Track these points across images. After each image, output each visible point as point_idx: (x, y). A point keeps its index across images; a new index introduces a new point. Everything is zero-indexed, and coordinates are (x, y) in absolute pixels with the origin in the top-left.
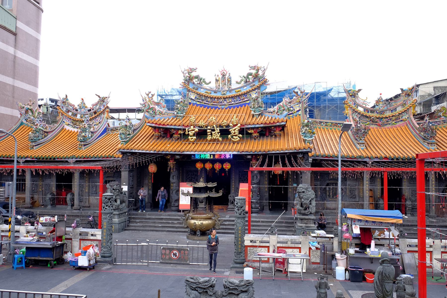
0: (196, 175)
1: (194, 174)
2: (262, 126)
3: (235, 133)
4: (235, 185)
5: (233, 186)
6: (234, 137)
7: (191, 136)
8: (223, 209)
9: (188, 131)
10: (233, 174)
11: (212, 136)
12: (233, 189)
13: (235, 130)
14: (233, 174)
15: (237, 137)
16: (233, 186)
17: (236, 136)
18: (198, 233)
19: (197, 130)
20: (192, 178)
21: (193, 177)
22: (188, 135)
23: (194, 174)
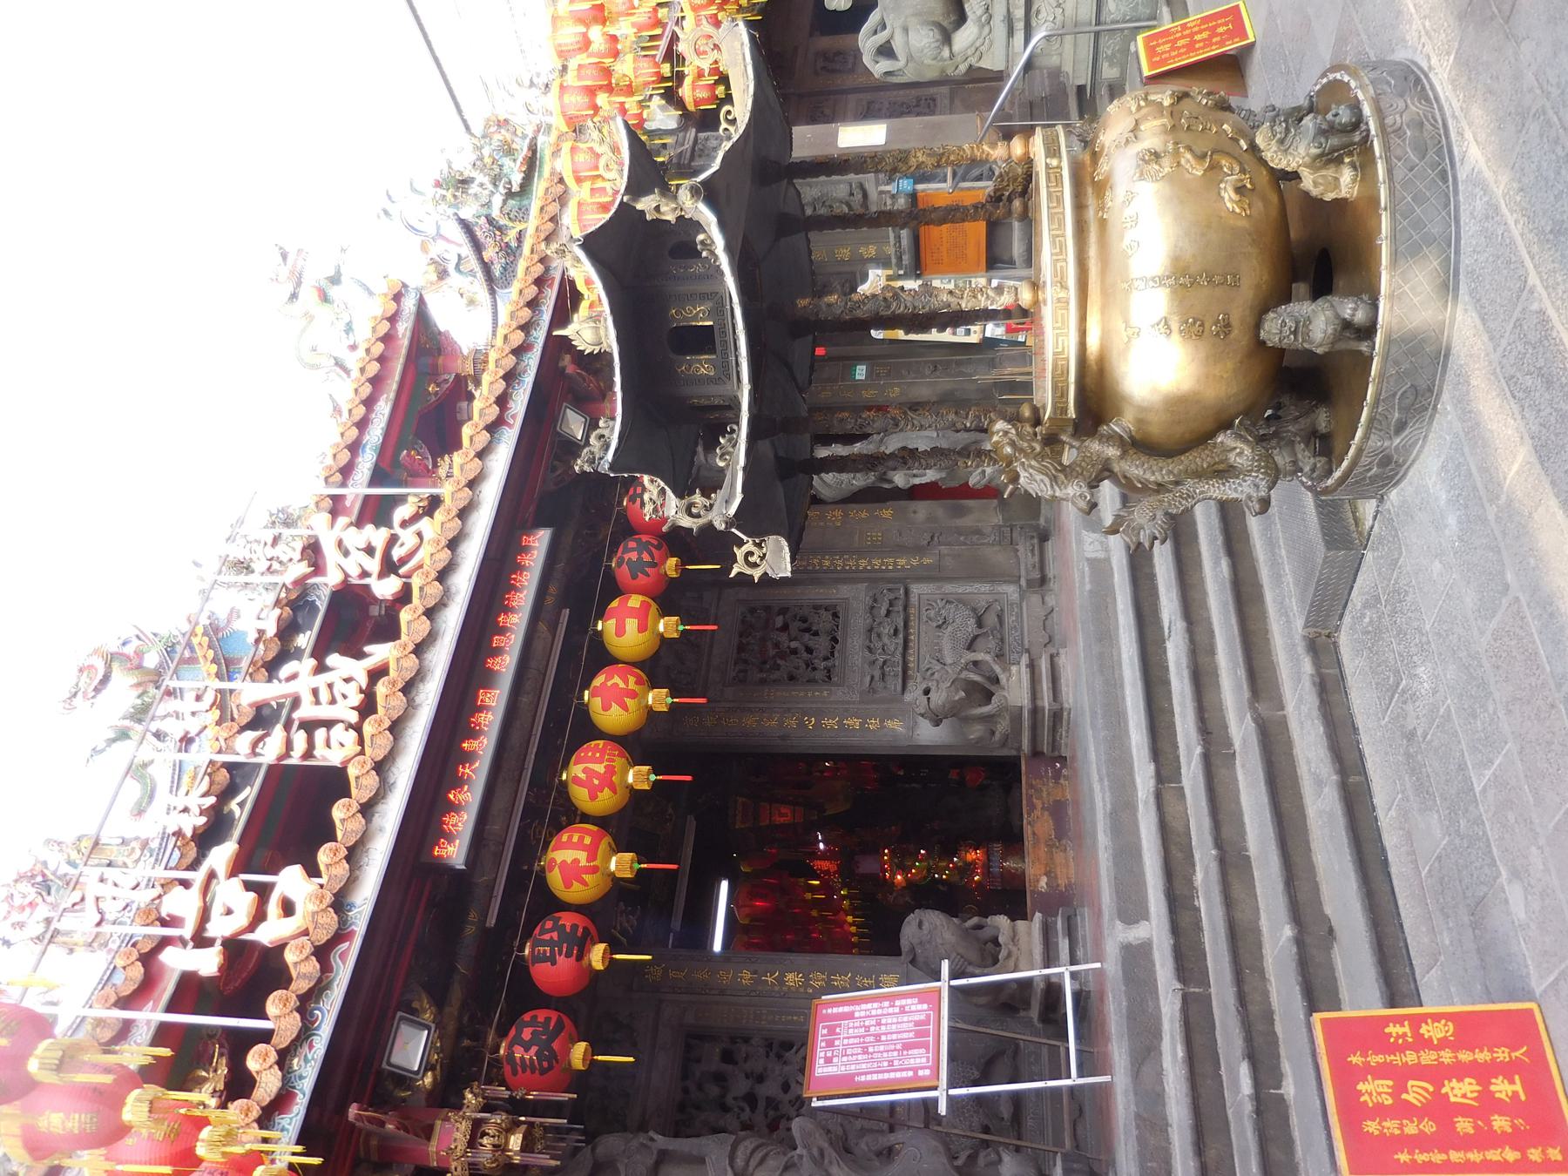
0: (728, 1057)
1: (720, 1078)
2: (383, 408)
3: (370, 550)
4: (847, 713)
5: (855, 723)
6: (397, 553)
7: (259, 916)
8: (1058, 811)
9: (201, 941)
10: (750, 721)
11: (329, 724)
12: (873, 724)
13: (351, 555)
14: (750, 721)
15: (408, 537)
16: (855, 723)
17: (393, 540)
18: (1314, 322)
19: (222, 855)
20: (751, 1099)
21: (741, 1086)
22: (235, 949)
23: (720, 1078)
